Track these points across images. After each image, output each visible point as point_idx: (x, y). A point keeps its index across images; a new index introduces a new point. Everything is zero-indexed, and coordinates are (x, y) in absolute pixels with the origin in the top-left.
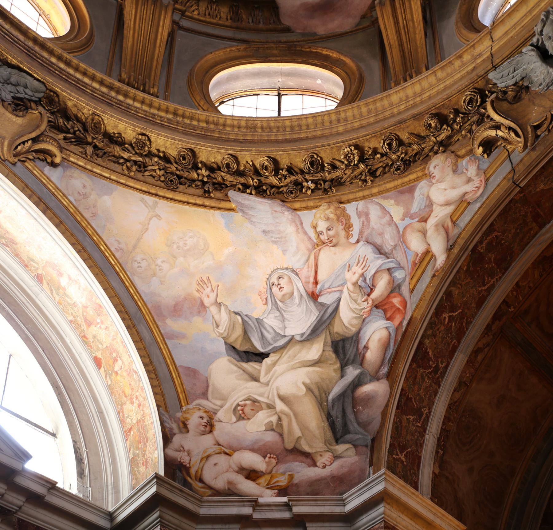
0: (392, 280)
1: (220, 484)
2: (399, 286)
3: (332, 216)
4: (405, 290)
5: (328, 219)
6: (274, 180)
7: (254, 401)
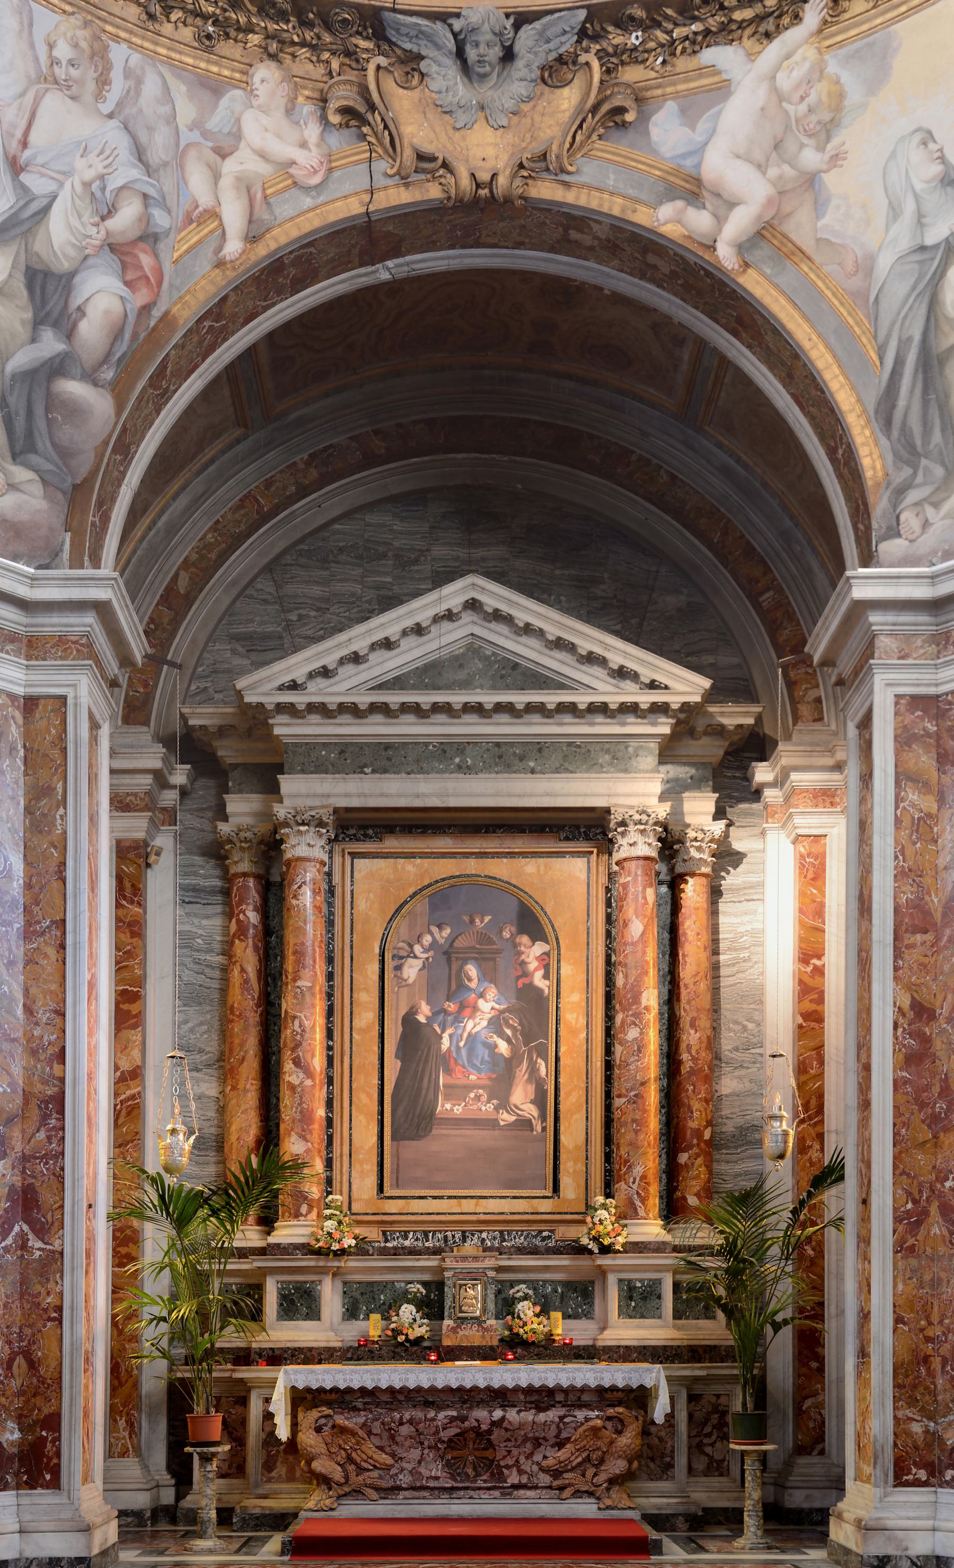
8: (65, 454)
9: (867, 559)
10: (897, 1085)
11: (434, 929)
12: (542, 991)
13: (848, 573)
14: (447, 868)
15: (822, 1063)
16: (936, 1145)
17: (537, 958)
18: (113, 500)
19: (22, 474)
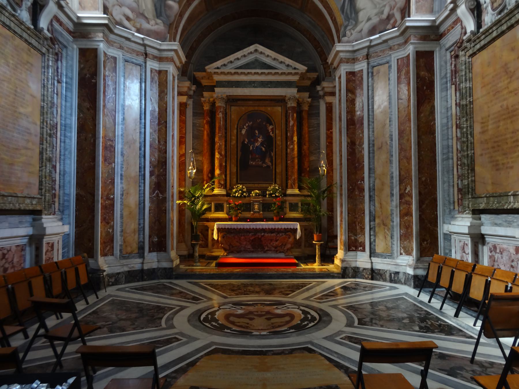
8: (168, 17)
9: (339, 41)
10: (348, 160)
11: (248, 122)
12: (272, 136)
13: (335, 45)
14: (251, 109)
15: (332, 153)
17: (271, 129)
19: (159, 21)
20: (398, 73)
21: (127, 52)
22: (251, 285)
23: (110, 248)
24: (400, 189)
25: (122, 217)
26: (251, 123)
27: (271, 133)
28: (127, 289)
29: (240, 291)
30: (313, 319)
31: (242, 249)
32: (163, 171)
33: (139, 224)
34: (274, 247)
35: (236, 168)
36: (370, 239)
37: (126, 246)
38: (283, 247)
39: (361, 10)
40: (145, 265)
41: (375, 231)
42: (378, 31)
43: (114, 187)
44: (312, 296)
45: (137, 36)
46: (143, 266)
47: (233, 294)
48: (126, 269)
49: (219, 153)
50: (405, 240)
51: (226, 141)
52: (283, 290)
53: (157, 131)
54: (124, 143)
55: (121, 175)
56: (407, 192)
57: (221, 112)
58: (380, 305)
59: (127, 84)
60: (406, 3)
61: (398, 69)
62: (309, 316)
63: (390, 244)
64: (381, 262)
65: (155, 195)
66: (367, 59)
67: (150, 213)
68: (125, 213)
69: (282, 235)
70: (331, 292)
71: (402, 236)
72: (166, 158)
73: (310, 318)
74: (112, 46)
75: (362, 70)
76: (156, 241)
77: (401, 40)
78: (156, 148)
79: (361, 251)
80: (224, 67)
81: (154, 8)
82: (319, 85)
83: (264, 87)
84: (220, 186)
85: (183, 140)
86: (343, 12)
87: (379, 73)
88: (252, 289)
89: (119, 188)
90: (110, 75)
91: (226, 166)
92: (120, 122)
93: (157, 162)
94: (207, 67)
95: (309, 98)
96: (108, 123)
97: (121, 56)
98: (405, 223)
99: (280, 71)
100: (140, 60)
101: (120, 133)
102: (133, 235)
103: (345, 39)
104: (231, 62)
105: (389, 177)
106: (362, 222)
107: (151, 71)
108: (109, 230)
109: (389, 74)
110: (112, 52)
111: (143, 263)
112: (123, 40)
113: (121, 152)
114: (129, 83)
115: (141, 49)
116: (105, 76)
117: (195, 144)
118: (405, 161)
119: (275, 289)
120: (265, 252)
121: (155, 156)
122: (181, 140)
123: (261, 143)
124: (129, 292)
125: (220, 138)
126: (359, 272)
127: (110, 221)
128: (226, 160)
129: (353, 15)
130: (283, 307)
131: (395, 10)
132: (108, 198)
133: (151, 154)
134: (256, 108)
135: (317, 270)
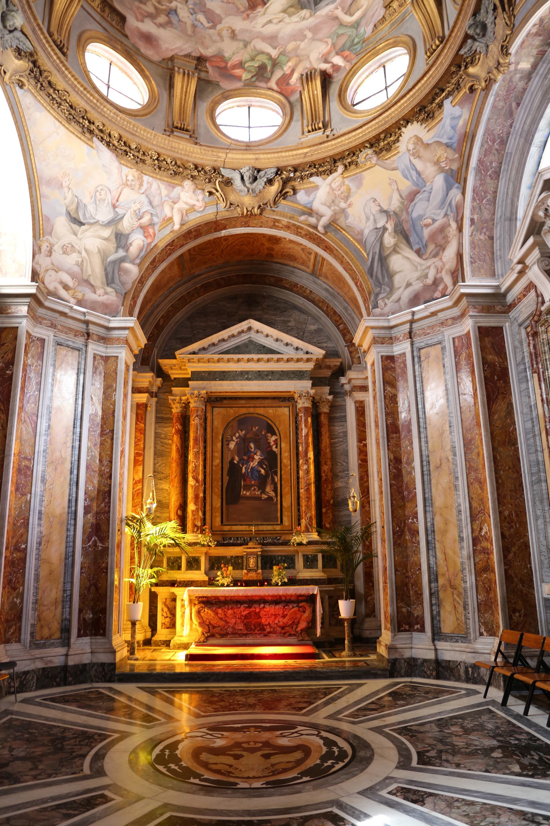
0: (151, 220)
1: (51, 287)
2: (154, 225)
3: (136, 176)
4: (157, 228)
5: (134, 176)
6: (116, 143)
7: (73, 246)
8: (123, 284)
16: (405, 507)
18: (138, 297)
19: (109, 290)
20: (455, 358)
21: (62, 332)
22: (242, 692)
23: (16, 630)
24: (473, 530)
25: (37, 579)
26: (244, 432)
27: (274, 447)
28: (38, 700)
29: (222, 703)
30: (343, 754)
31: (230, 630)
32: (105, 506)
33: (64, 591)
34: (279, 627)
35: (220, 501)
36: (432, 611)
37: (42, 627)
38: (294, 628)
39: (396, 273)
40: (70, 658)
41: (438, 598)
42: (422, 300)
43: (28, 531)
44: (340, 712)
45: (76, 310)
46: (66, 661)
47: (210, 708)
48: (39, 665)
49: (193, 477)
50: (486, 611)
51: (205, 460)
52: (293, 701)
53: (99, 445)
54: (47, 464)
55: (40, 512)
56: (483, 534)
57: (197, 416)
58: (452, 725)
59: (58, 375)
60: (457, 264)
61: (455, 352)
62: (335, 749)
63: (463, 618)
64: (450, 648)
65: (91, 543)
66: (411, 338)
67: (81, 573)
68: (43, 573)
69: (293, 607)
70: (372, 703)
71: (481, 604)
72: (110, 485)
73: (337, 753)
74: (41, 323)
75: (404, 354)
76: (89, 619)
77: (456, 311)
78: (95, 471)
79: (419, 631)
80: (204, 352)
81: (104, 273)
82: (343, 376)
83: (263, 379)
84: (195, 530)
85: (141, 458)
86: (372, 276)
87: (429, 357)
88: (242, 699)
89: (36, 532)
90: (33, 364)
91: (205, 498)
92: (44, 432)
93: (96, 493)
94: (177, 353)
95: (330, 394)
96: (24, 432)
97: (52, 337)
98: (483, 584)
99: (285, 357)
100: (79, 342)
101: (42, 448)
102: (53, 608)
103: (377, 311)
104: (214, 345)
105: (454, 511)
106: (418, 583)
107: (94, 357)
108: (15, 600)
109: (443, 359)
110: (39, 332)
111: (67, 655)
112: (57, 315)
113: (42, 477)
114: (61, 375)
115: (82, 327)
116: (25, 365)
117: (157, 465)
118: (476, 485)
119: (279, 700)
120: (265, 635)
121: (93, 483)
122: (137, 458)
123: (258, 463)
124: (40, 704)
125: (196, 454)
126: (416, 665)
127: (18, 585)
128: (205, 488)
129: (386, 279)
130: (293, 733)
131: (444, 272)
132: (17, 549)
133: (88, 480)
134: (252, 410)
135: (347, 664)
